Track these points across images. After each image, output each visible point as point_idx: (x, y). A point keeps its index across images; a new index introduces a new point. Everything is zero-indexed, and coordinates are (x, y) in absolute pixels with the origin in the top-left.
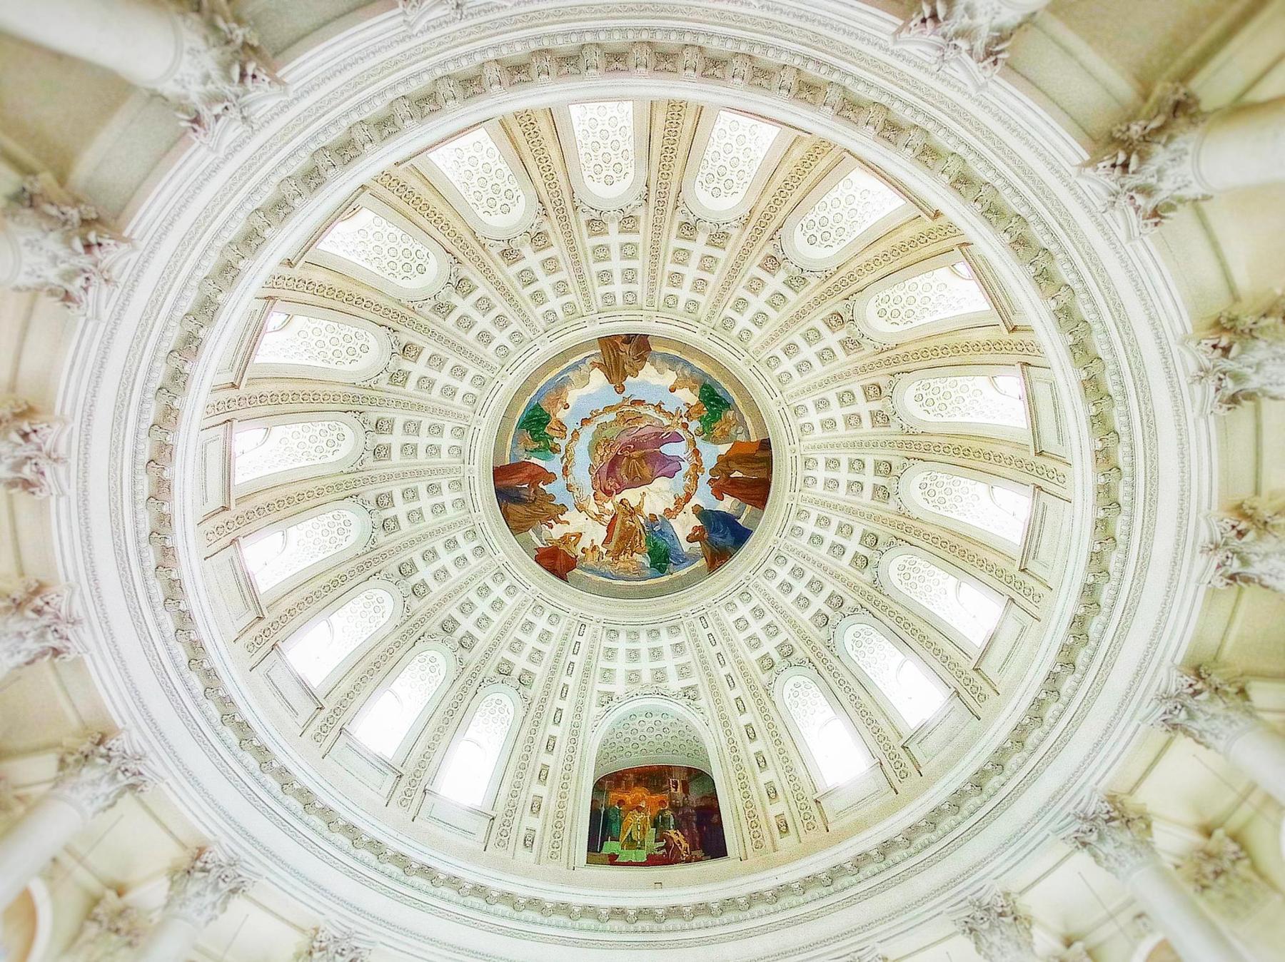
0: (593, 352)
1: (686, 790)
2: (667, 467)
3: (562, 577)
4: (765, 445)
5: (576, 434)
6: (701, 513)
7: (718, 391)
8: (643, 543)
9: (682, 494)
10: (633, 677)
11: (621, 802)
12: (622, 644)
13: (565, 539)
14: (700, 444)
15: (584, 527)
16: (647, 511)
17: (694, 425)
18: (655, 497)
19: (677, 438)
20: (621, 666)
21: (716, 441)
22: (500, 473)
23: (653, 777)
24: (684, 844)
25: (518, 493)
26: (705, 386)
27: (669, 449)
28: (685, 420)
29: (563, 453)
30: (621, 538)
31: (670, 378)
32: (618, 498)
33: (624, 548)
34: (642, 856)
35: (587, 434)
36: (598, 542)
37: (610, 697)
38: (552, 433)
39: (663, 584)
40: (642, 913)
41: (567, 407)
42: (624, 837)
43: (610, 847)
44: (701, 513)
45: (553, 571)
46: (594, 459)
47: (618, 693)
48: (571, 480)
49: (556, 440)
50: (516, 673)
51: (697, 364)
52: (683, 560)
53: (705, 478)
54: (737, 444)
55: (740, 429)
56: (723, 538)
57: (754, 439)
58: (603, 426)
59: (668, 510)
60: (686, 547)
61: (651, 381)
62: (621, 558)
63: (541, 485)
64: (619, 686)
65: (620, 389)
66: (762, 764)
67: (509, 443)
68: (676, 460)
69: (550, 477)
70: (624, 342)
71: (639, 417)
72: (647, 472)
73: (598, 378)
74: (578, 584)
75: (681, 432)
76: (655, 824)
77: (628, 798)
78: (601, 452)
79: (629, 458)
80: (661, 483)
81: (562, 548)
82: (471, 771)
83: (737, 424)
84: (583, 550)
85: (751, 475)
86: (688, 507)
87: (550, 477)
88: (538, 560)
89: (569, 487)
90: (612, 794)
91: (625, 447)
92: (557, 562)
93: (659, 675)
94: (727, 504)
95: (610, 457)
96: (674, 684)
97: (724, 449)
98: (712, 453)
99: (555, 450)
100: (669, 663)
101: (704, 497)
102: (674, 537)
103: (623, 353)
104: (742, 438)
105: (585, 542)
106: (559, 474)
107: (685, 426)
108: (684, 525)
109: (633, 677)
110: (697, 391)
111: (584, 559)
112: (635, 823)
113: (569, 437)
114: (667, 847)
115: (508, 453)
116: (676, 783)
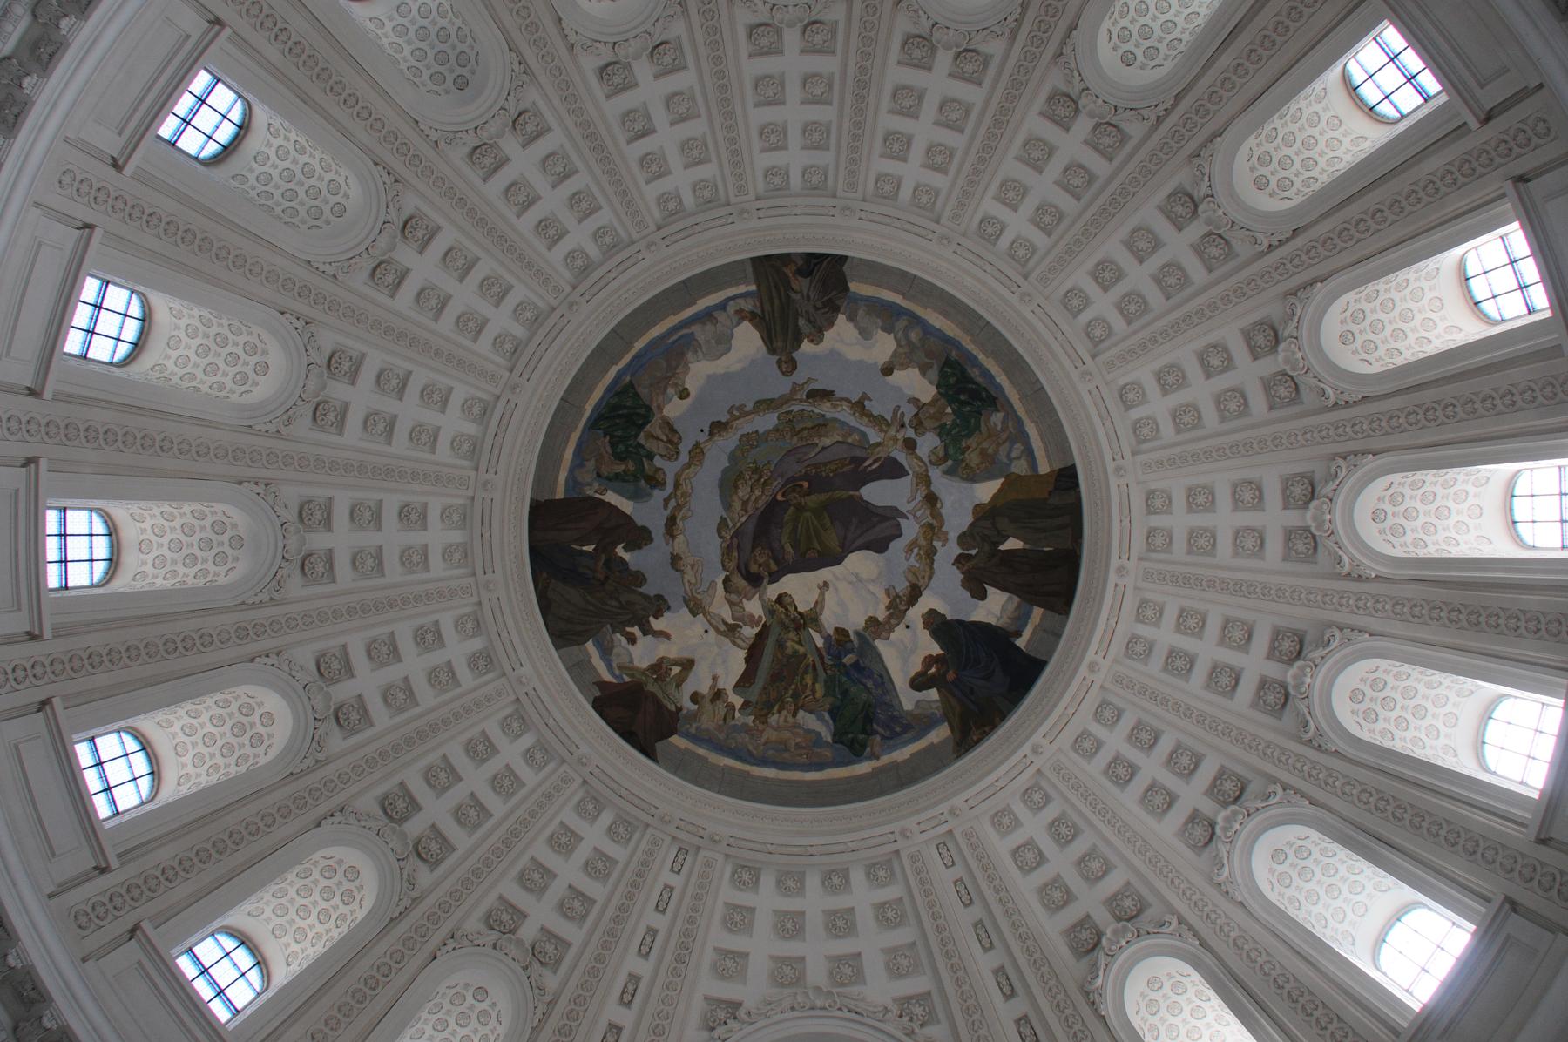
0: (742, 289)
2: (876, 530)
3: (649, 753)
4: (1067, 478)
5: (697, 452)
6: (937, 625)
7: (974, 373)
8: (820, 689)
9: (902, 587)
10: (788, 973)
12: (766, 899)
13: (659, 668)
14: (942, 484)
15: (701, 648)
16: (829, 620)
17: (928, 443)
18: (845, 593)
19: (892, 470)
20: (762, 945)
21: (972, 478)
22: (542, 514)
25: (580, 565)
26: (948, 363)
27: (876, 493)
28: (910, 433)
29: (670, 488)
30: (775, 677)
31: (884, 346)
32: (773, 591)
33: (780, 699)
35: (719, 454)
36: (728, 683)
38: (651, 445)
39: (860, 778)
41: (684, 394)
44: (937, 625)
45: (628, 736)
46: (727, 506)
47: (749, 1004)
48: (680, 544)
49: (658, 462)
51: (936, 320)
52: (906, 727)
53: (948, 551)
54: (1012, 481)
55: (1018, 449)
56: (988, 681)
57: (1044, 468)
58: (750, 441)
59: (872, 622)
60: (909, 700)
61: (847, 348)
62: (773, 719)
63: (619, 550)
65: (788, 365)
67: (569, 454)
68: (891, 516)
69: (639, 537)
70: (800, 272)
71: (822, 425)
72: (832, 540)
73: (747, 341)
74: (683, 767)
75: (901, 457)
78: (743, 492)
79: (800, 508)
80: (860, 563)
81: (652, 687)
83: (1012, 440)
84: (695, 698)
85: (1040, 542)
86: (916, 614)
87: (639, 537)
88: (599, 706)
89: (675, 560)
91: (792, 484)
92: (639, 714)
93: (848, 969)
94: (994, 608)
95: (761, 503)
96: (879, 989)
97: (986, 491)
98: (964, 499)
99: (655, 481)
100: (871, 942)
101: (946, 595)
102: (884, 680)
103: (798, 291)
104: (1020, 468)
105: (700, 681)
106: (658, 531)
107: (910, 445)
108: (906, 653)
109: (788, 973)
110: (934, 373)
111: (694, 716)
113: (684, 457)
115: (562, 476)
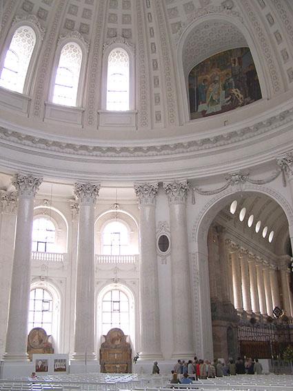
1: (240, 64)
11: (205, 80)
23: (220, 60)
24: (240, 96)
34: (219, 108)
37: (179, 24)
40: (217, 139)
42: (208, 100)
43: (202, 107)
50: (119, 32)
64: (182, 17)
66: (279, 38)
76: (224, 88)
77: (208, 77)
82: (119, 92)
90: (199, 78)
112: (215, 91)
114: (232, 99)
116: (235, 60)
